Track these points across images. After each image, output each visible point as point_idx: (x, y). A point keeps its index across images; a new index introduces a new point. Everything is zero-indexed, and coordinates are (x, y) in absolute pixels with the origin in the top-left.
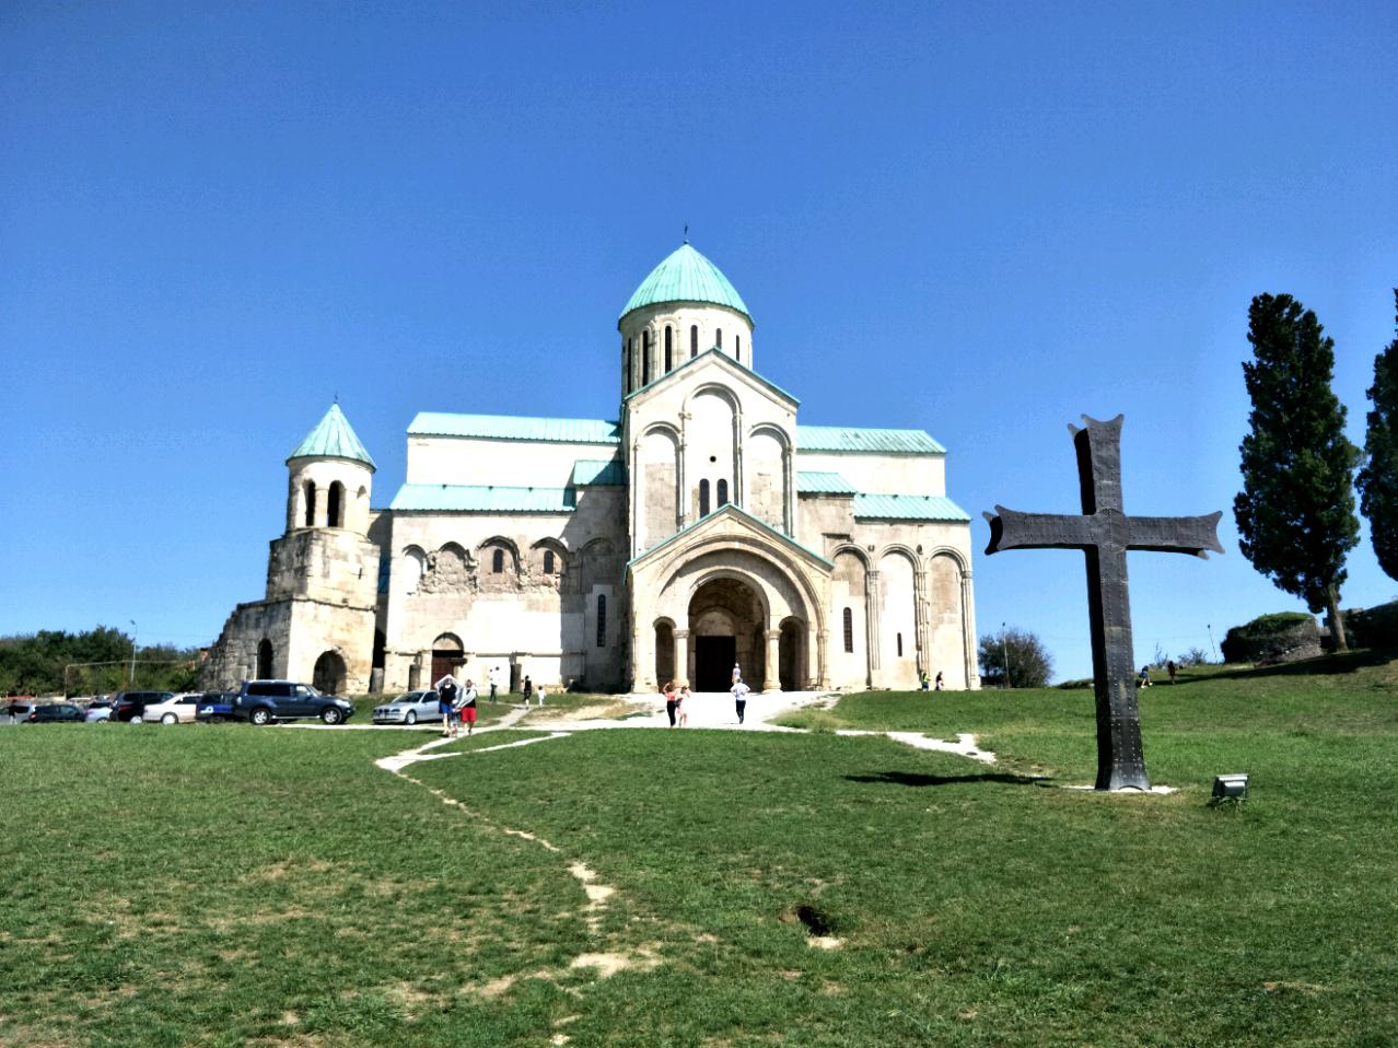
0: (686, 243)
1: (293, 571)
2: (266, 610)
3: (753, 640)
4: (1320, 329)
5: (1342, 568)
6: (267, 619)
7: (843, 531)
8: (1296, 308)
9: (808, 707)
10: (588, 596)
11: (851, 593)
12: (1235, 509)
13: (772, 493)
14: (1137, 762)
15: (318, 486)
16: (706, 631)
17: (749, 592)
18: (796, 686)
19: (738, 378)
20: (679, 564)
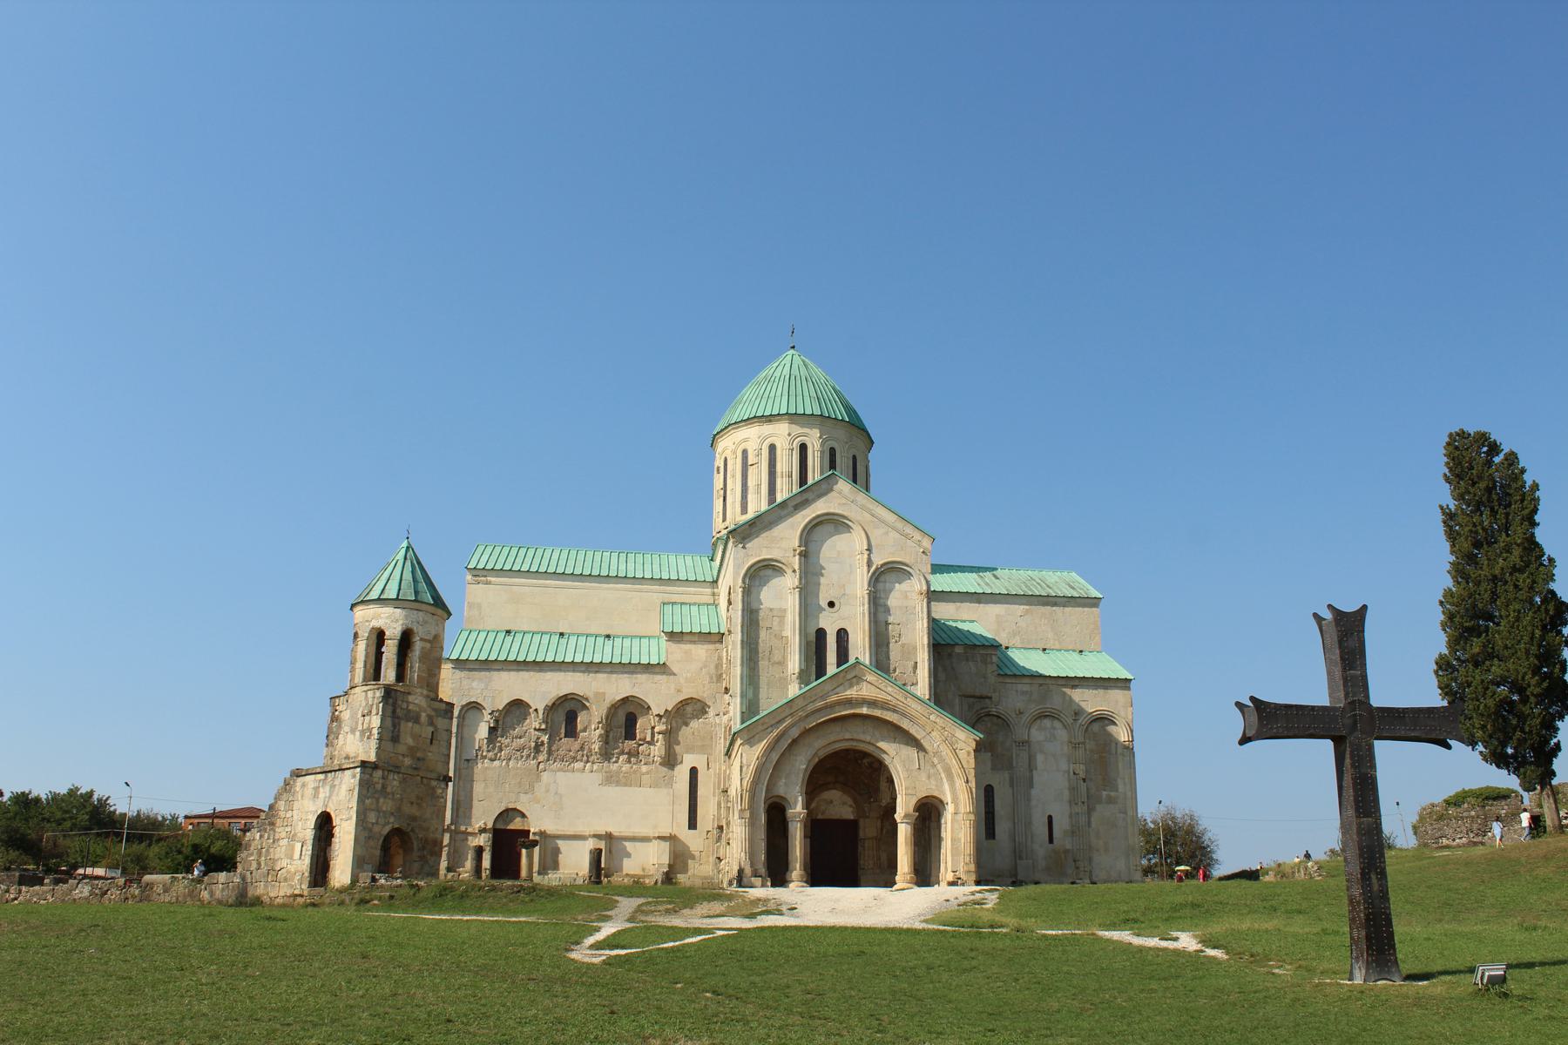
0: (793, 347)
1: (358, 733)
2: (326, 777)
3: (879, 823)
4: (1523, 471)
5: (1555, 740)
6: (328, 788)
7: (985, 693)
8: (1494, 448)
9: (965, 904)
10: (678, 768)
11: (994, 768)
12: (1436, 672)
13: (903, 646)
14: (1389, 954)
15: (387, 633)
16: (823, 813)
17: (876, 765)
18: (933, 879)
19: (863, 508)
20: (795, 733)
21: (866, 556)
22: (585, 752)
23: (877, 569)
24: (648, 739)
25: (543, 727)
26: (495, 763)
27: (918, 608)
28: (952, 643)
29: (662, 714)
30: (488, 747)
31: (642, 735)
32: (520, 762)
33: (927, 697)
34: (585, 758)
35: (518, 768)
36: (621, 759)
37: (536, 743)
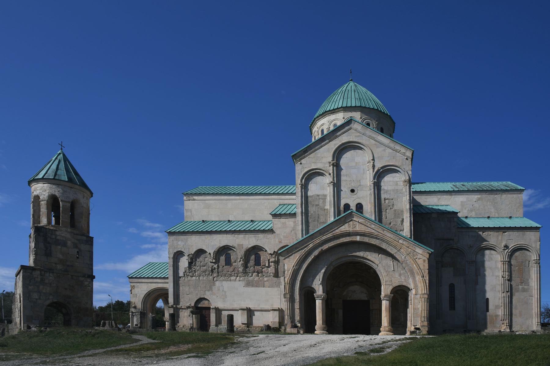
20: (316, 253)
21: (372, 163)
22: (236, 272)
23: (378, 170)
24: (267, 265)
25: (214, 261)
26: (194, 278)
27: (404, 190)
28: (429, 212)
29: (272, 253)
30: (189, 270)
31: (264, 264)
32: (205, 278)
33: (409, 236)
34: (236, 275)
35: (204, 280)
36: (254, 275)
37: (212, 268)
